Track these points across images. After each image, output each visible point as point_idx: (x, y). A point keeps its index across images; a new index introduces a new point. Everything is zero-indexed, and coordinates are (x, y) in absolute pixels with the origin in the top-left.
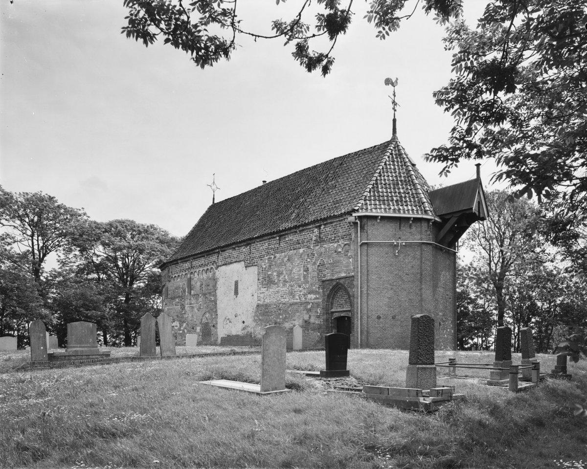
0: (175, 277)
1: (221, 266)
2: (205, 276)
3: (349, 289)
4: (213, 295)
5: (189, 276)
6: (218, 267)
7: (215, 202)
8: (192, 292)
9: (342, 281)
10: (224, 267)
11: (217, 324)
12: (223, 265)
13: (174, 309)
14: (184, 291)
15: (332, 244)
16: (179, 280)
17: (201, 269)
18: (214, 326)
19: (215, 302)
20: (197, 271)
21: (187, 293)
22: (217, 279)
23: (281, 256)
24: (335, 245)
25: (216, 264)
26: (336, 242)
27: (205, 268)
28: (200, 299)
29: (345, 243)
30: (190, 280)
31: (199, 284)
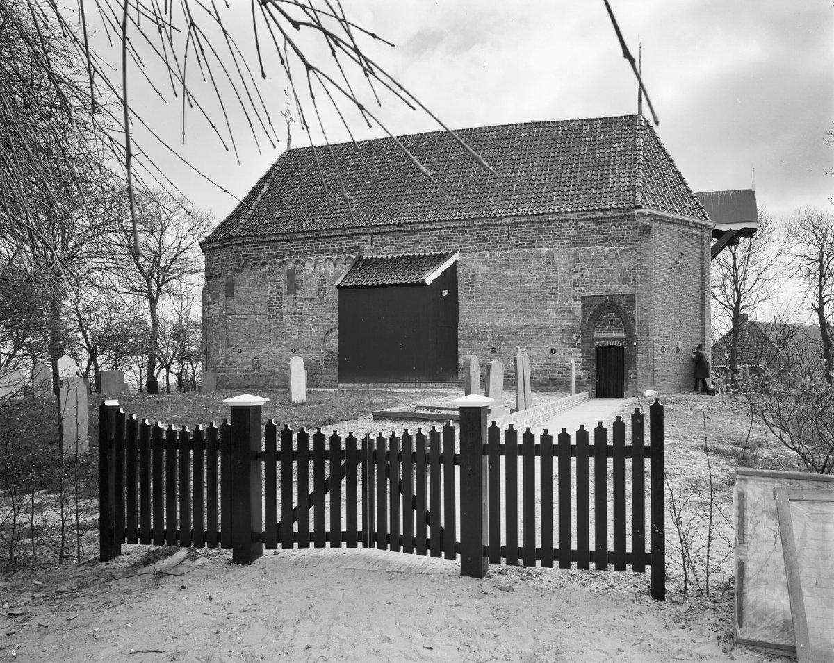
2: (330, 268)
3: (627, 311)
5: (290, 266)
7: (293, 146)
9: (616, 300)
15: (600, 247)
17: (324, 257)
20: (313, 259)
23: (504, 254)
24: (606, 249)
26: (606, 245)
27: (334, 257)
29: (623, 248)
30: (292, 274)
31: (315, 281)
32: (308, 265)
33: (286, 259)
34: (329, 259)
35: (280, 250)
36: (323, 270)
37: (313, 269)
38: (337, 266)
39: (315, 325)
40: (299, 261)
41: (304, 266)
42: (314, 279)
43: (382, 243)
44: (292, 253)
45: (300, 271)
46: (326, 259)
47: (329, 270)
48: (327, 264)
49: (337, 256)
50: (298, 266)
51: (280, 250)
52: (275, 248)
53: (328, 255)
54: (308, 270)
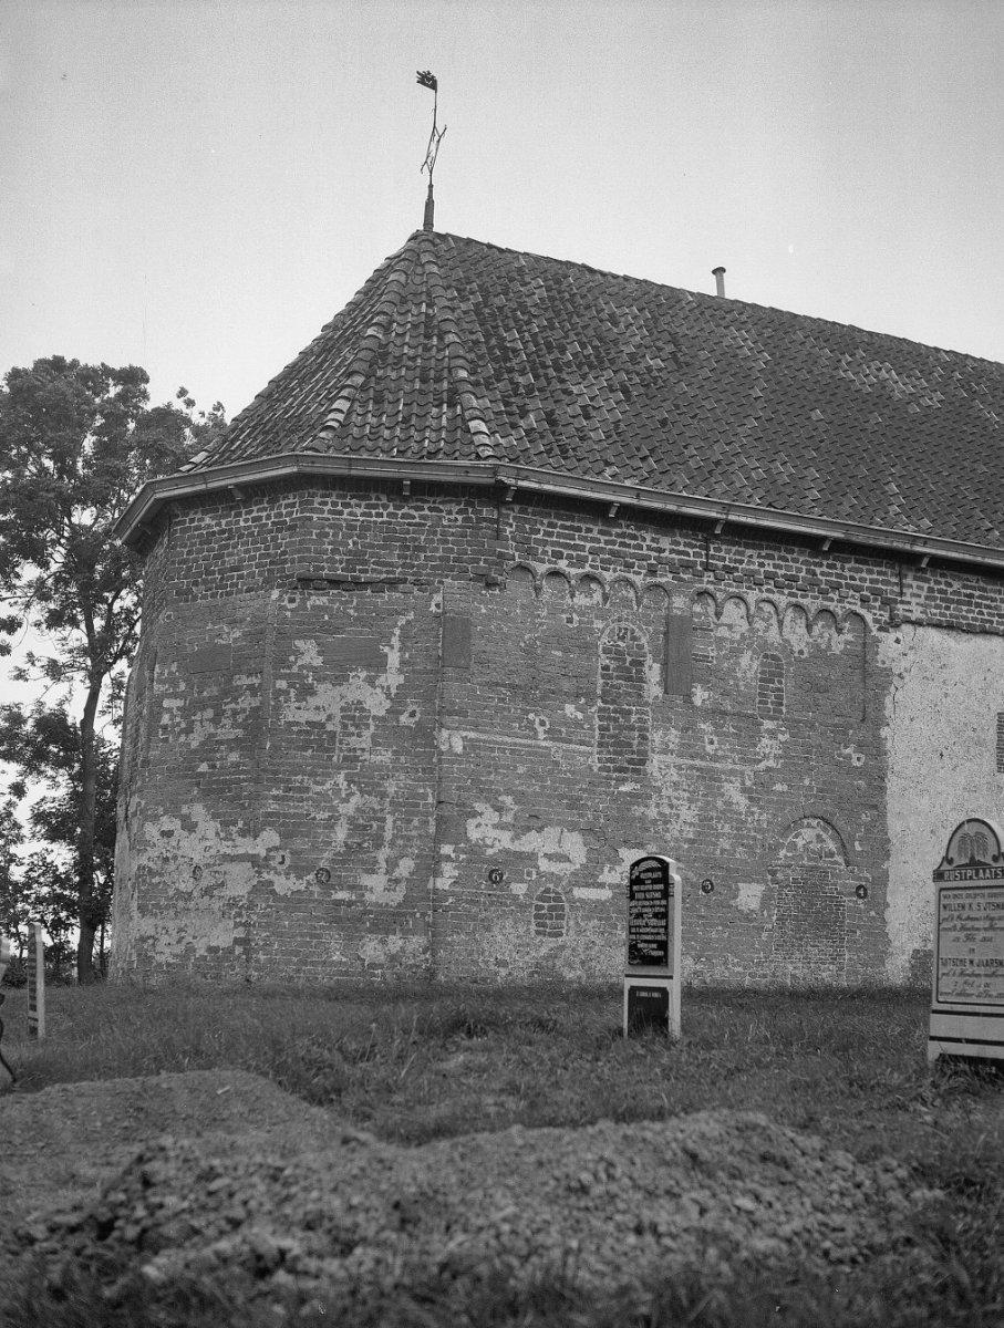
0: (555, 574)
1: (918, 623)
2: (797, 636)
4: (860, 746)
6: (894, 623)
8: (700, 696)
10: (934, 636)
11: (883, 880)
12: (938, 626)
13: (545, 754)
14: (632, 673)
16: (581, 600)
18: (861, 892)
19: (877, 778)
21: (653, 690)
22: (888, 672)
25: (886, 603)
27: (811, 603)
28: (766, 744)
30: (675, 633)
31: (749, 665)
32: (733, 612)
33: (666, 579)
34: (798, 607)
35: (649, 548)
36: (773, 635)
37: (746, 626)
38: (816, 630)
39: (750, 799)
40: (702, 594)
41: (718, 614)
42: (745, 660)
43: (945, 592)
44: (687, 566)
45: (706, 629)
46: (790, 605)
47: (793, 639)
48: (787, 620)
49: (820, 603)
50: (697, 608)
51: (649, 548)
52: (634, 537)
53: (794, 595)
54: (730, 627)
